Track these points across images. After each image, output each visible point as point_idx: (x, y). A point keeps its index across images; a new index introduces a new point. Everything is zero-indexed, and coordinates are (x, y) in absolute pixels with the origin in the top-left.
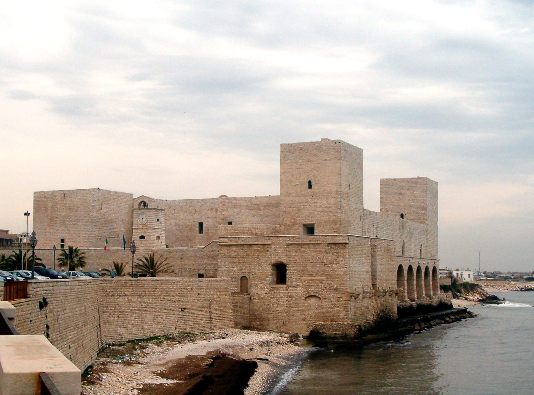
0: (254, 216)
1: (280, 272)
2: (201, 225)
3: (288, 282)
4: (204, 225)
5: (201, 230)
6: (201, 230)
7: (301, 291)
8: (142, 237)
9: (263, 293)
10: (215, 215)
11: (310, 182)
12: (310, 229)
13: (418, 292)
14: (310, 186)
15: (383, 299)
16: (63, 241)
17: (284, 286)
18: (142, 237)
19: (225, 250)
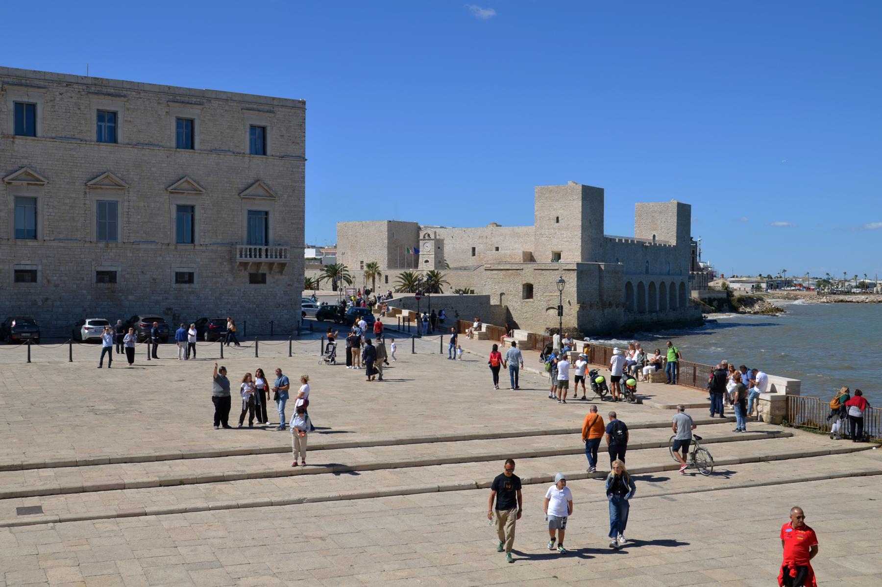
0: (516, 242)
1: (529, 291)
2: (474, 249)
3: (534, 297)
4: (476, 250)
5: (474, 254)
6: (474, 254)
7: (544, 305)
8: (427, 261)
9: (516, 305)
10: (485, 240)
11: (558, 218)
12: (557, 256)
13: (660, 305)
14: (558, 221)
15: (610, 310)
16: (362, 262)
17: (531, 300)
18: (427, 261)
19: (489, 272)
